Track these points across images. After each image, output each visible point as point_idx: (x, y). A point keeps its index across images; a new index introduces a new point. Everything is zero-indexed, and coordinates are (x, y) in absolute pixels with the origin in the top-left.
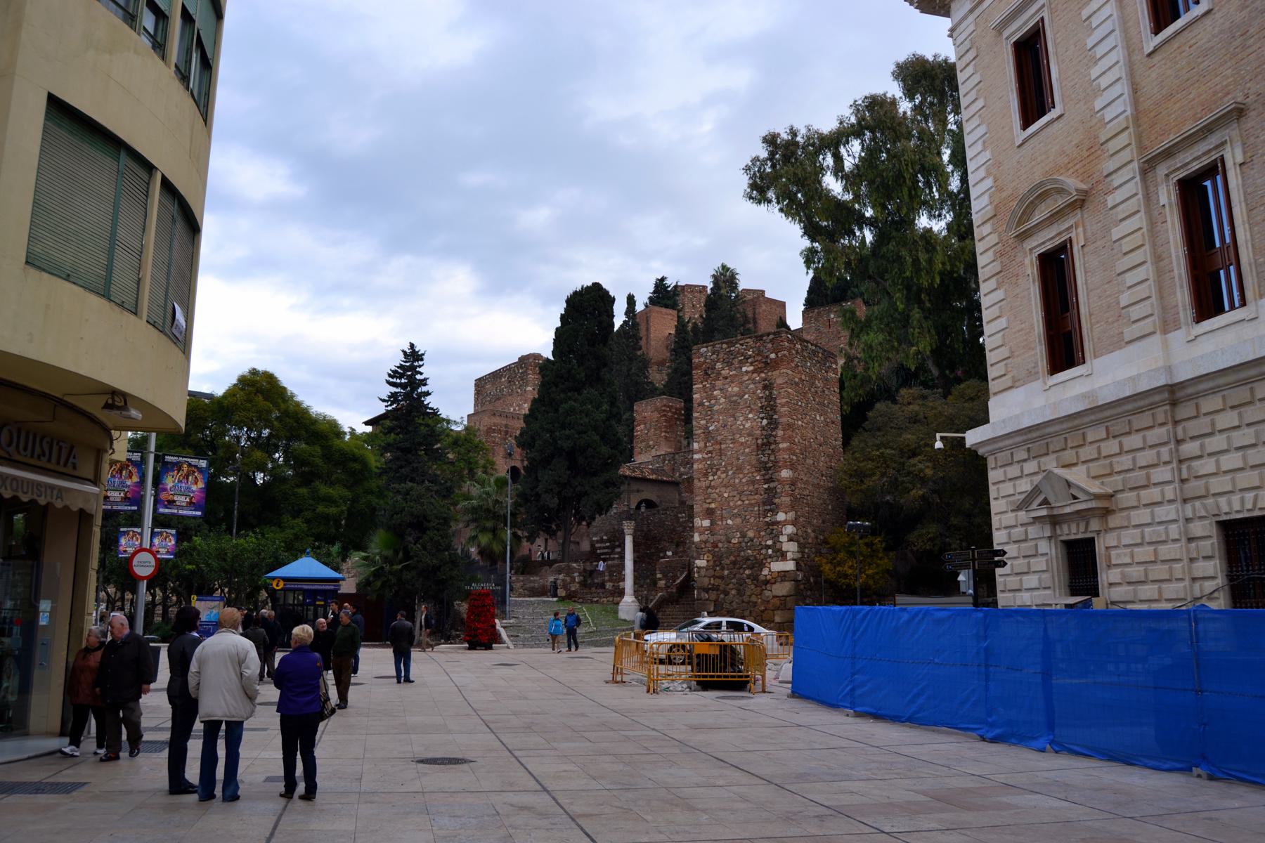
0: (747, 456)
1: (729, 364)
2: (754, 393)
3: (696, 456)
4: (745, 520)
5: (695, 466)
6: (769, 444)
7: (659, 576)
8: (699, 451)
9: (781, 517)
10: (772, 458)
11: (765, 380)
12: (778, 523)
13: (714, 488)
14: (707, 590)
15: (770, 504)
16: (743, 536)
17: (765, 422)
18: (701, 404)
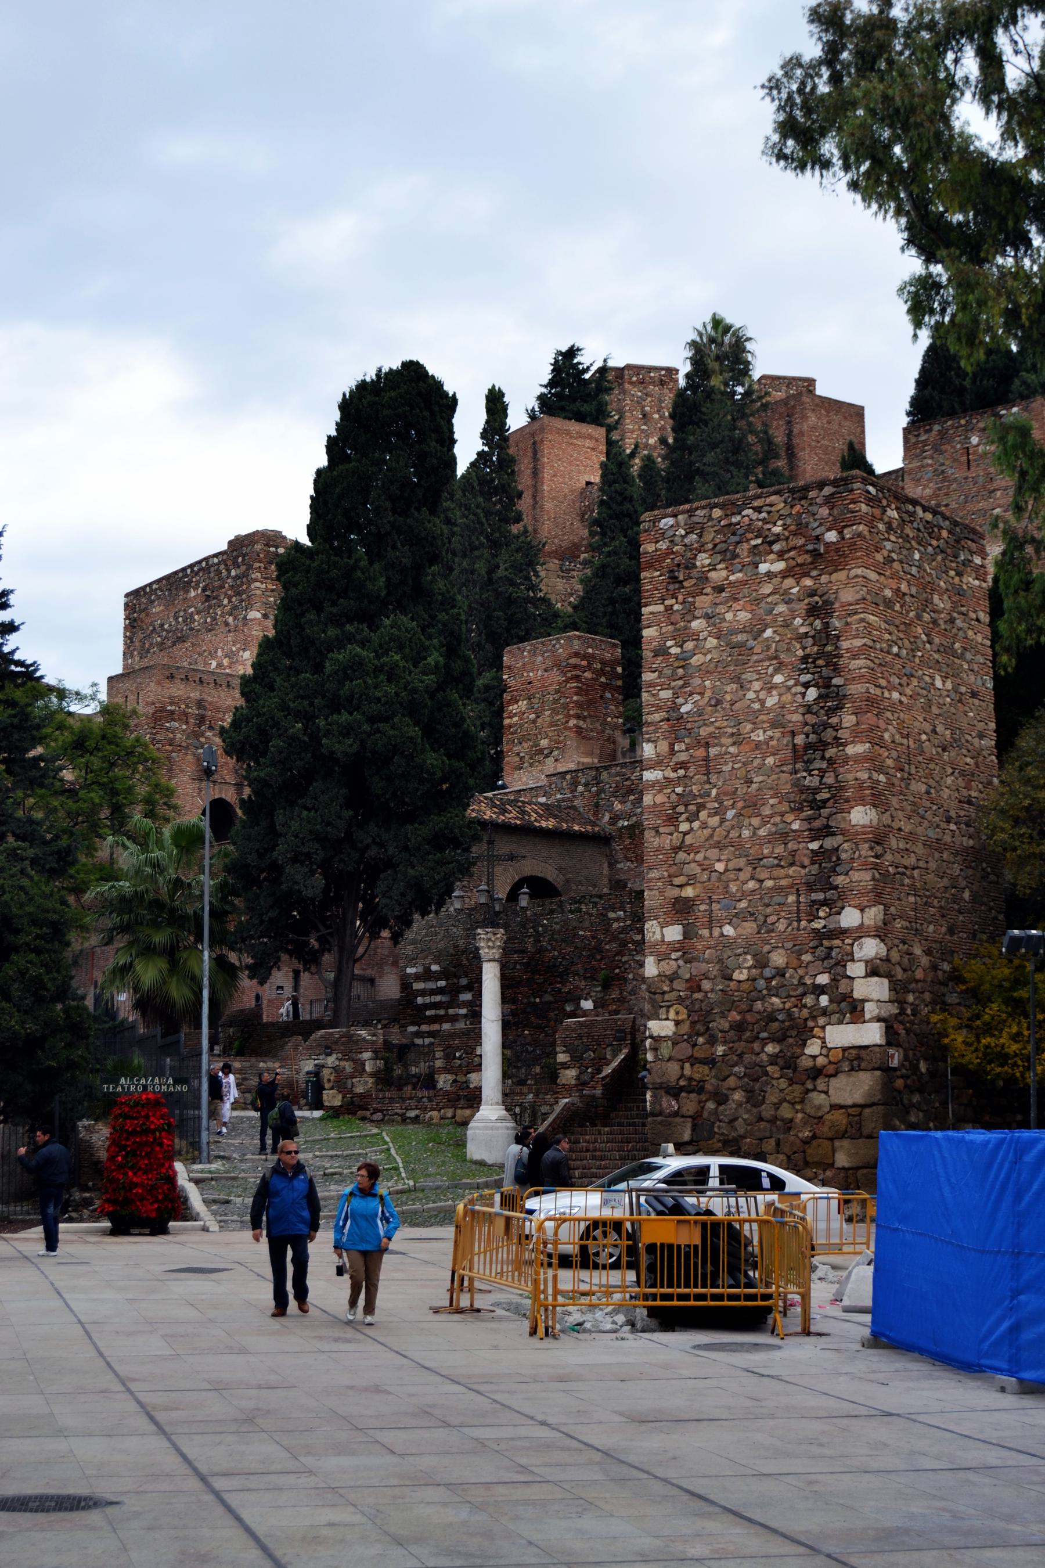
0: (770, 774)
1: (729, 556)
2: (787, 625)
3: (649, 776)
4: (765, 927)
5: (648, 799)
6: (822, 745)
7: (562, 1058)
8: (658, 763)
9: (850, 918)
10: (829, 779)
11: (812, 593)
12: (843, 932)
13: (691, 849)
14: (675, 1092)
15: (824, 887)
16: (761, 962)
17: (812, 693)
18: (661, 652)
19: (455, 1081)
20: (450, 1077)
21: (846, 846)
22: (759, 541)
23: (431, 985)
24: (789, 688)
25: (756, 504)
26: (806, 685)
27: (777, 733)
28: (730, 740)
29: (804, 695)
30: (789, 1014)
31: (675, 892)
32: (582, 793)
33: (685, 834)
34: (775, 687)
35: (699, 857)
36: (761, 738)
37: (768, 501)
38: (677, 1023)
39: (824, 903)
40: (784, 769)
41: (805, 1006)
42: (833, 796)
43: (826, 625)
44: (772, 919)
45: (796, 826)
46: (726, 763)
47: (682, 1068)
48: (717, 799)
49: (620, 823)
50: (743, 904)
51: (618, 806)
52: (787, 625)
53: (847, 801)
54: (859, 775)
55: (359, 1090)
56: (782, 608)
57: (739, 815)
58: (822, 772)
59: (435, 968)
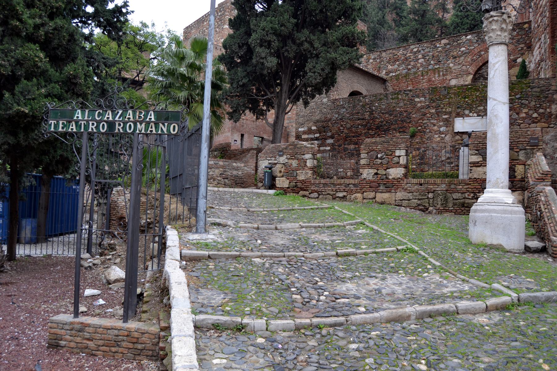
19: (376, 174)
20: (373, 171)
23: (312, 136)
32: (372, 63)
49: (391, 74)
51: (390, 67)
55: (301, 177)
59: (314, 128)
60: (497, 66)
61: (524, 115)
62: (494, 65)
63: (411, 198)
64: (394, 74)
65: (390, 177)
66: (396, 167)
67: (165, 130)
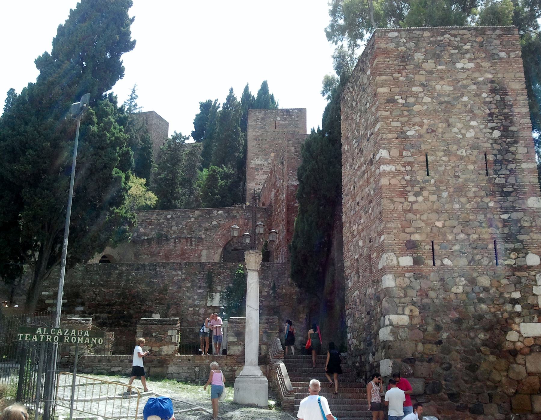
0: (471, 173)
2: (477, 95)
10: (512, 180)
11: (492, 82)
12: (529, 268)
16: (472, 282)
17: (497, 134)
18: (391, 101)
21: (526, 218)
22: (456, 51)
24: (481, 130)
25: (453, 32)
26: (493, 129)
27: (475, 152)
28: (443, 153)
29: (491, 133)
30: (495, 315)
31: (408, 237)
33: (412, 203)
34: (473, 127)
35: (424, 217)
36: (464, 154)
37: (461, 32)
38: (411, 317)
39: (514, 250)
40: (481, 172)
41: (506, 311)
42: (515, 190)
43: (502, 99)
44: (478, 257)
45: (491, 204)
46: (441, 166)
47: (416, 346)
48: (435, 184)
50: (457, 247)
52: (477, 95)
53: (525, 193)
54: (532, 180)
56: (474, 87)
57: (450, 196)
58: (507, 177)
60: (252, 285)
61: (266, 294)
62: (251, 284)
63: (181, 371)
64: (146, 238)
65: (163, 354)
66: (168, 345)
67: (95, 342)
